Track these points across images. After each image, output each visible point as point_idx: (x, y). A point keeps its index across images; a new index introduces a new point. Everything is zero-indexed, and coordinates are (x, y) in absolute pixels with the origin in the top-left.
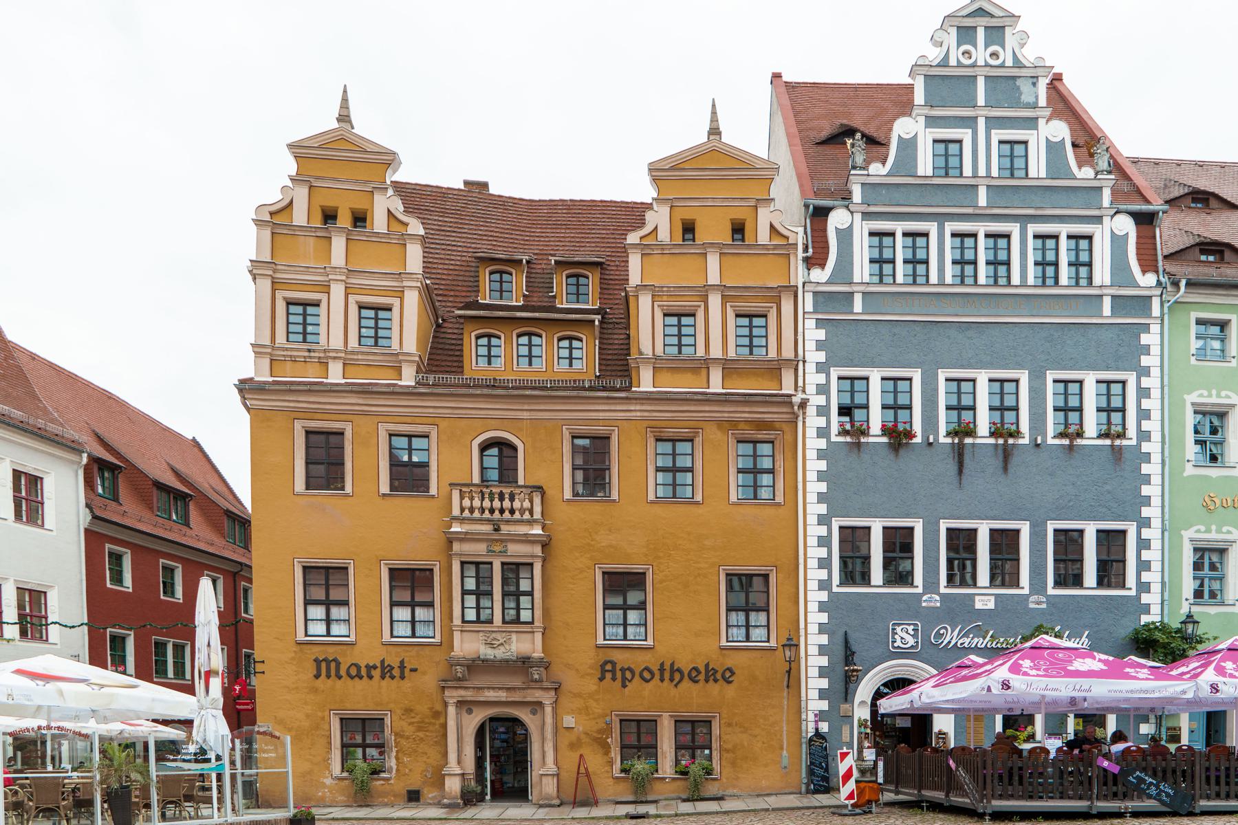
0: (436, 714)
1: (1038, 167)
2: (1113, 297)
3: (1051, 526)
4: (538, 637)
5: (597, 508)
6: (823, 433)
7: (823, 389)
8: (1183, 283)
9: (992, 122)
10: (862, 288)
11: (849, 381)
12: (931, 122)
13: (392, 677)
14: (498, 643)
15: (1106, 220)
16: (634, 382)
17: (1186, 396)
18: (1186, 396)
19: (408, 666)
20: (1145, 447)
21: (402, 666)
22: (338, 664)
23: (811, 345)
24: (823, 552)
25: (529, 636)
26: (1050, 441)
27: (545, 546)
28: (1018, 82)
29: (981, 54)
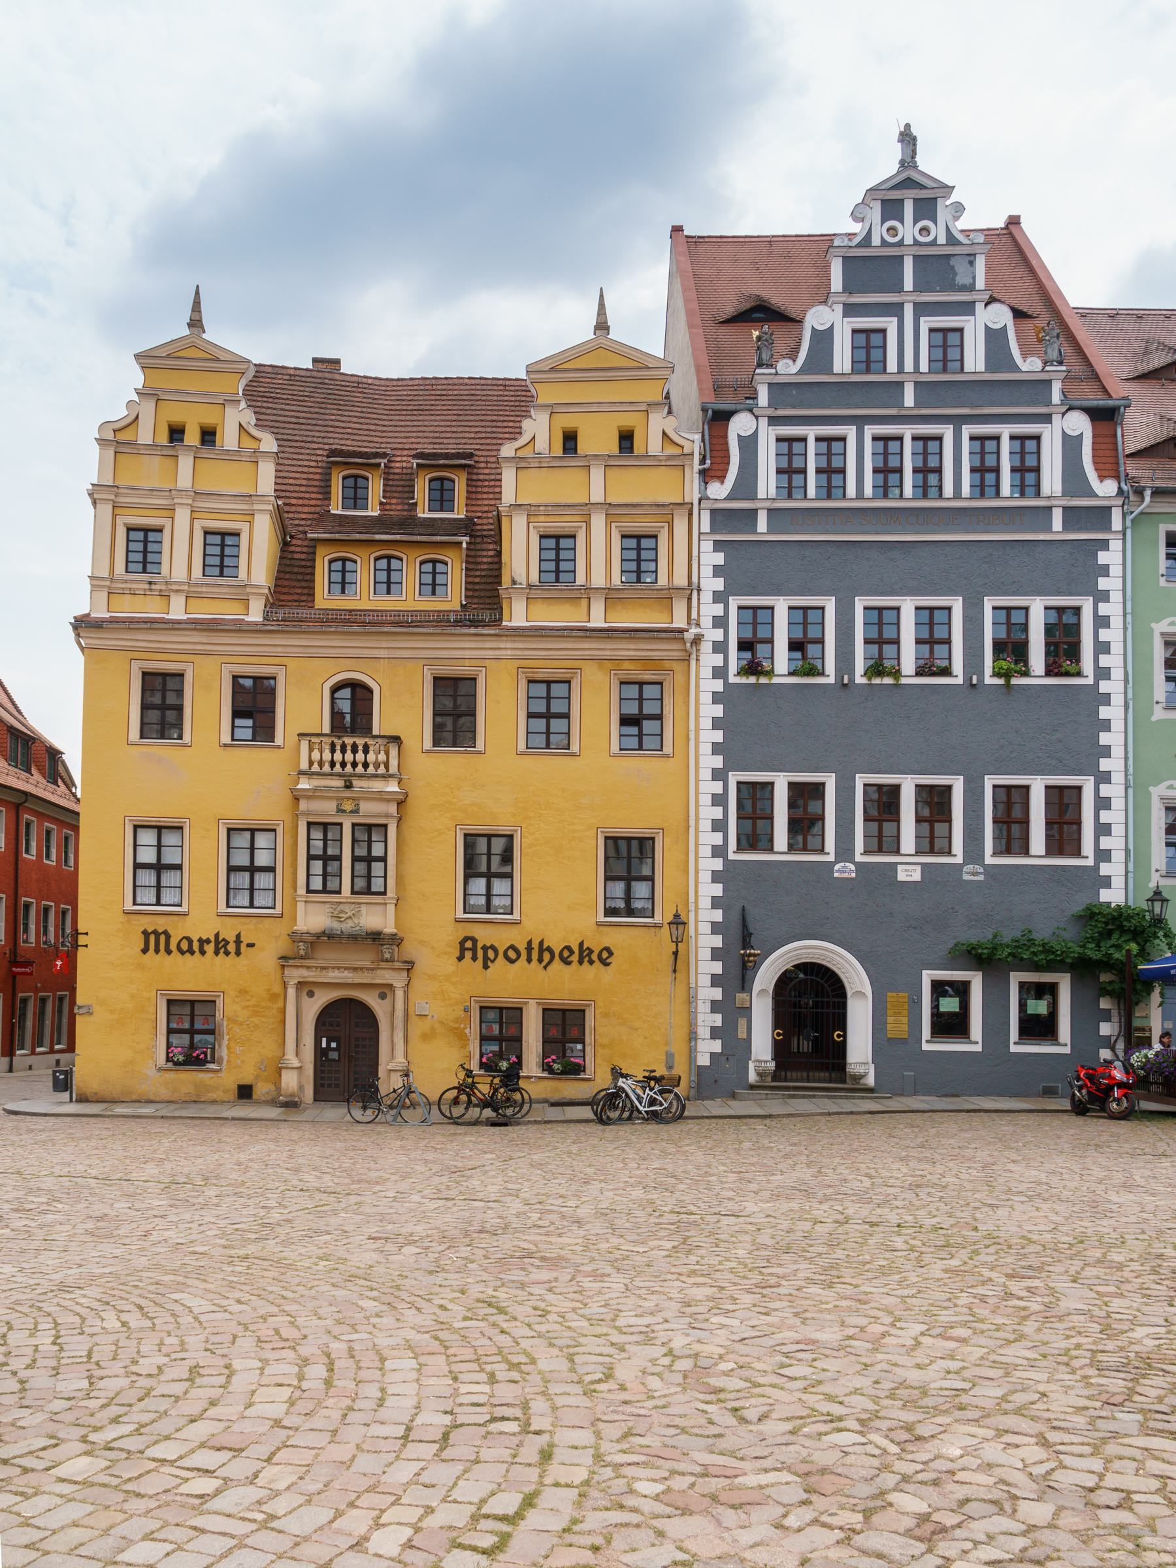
0: (273, 997)
1: (975, 359)
2: (1064, 508)
3: (989, 782)
4: (391, 908)
5: (460, 759)
6: (719, 672)
7: (720, 622)
8: (1148, 493)
9: (921, 309)
10: (767, 504)
11: (751, 611)
12: (850, 310)
13: (227, 953)
14: (346, 916)
15: (1056, 419)
16: (505, 616)
17: (1153, 625)
18: (1153, 625)
19: (245, 940)
20: (1104, 687)
21: (238, 941)
22: (168, 937)
23: (707, 571)
24: (718, 813)
25: (381, 908)
26: (989, 680)
27: (400, 804)
28: (953, 262)
29: (908, 231)
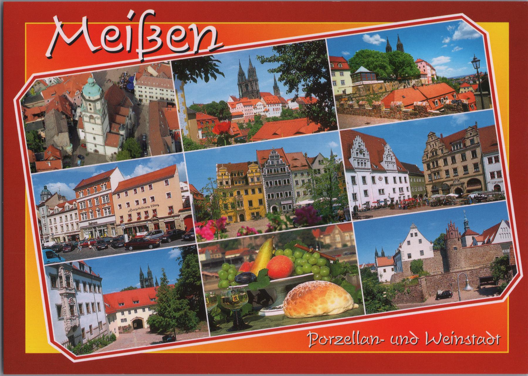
29: (274, 154)
